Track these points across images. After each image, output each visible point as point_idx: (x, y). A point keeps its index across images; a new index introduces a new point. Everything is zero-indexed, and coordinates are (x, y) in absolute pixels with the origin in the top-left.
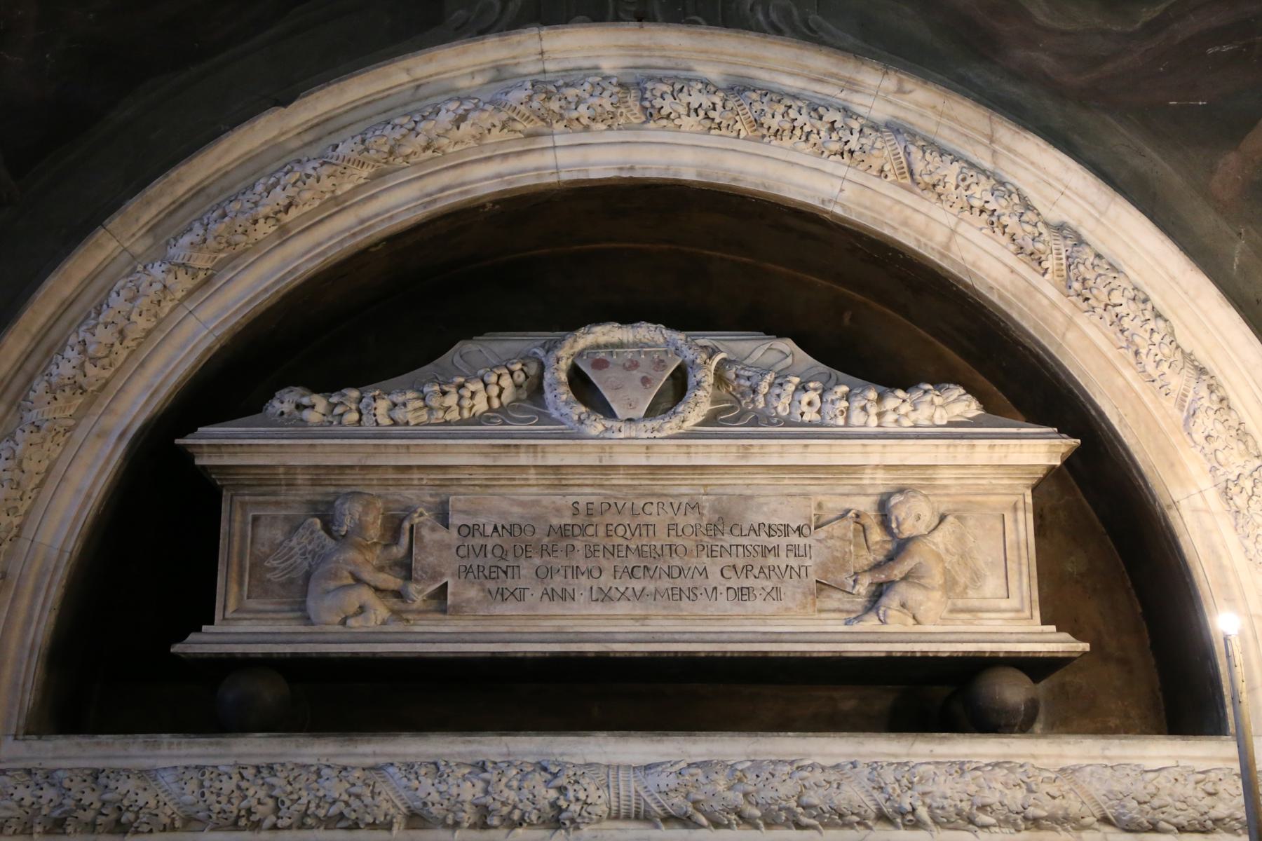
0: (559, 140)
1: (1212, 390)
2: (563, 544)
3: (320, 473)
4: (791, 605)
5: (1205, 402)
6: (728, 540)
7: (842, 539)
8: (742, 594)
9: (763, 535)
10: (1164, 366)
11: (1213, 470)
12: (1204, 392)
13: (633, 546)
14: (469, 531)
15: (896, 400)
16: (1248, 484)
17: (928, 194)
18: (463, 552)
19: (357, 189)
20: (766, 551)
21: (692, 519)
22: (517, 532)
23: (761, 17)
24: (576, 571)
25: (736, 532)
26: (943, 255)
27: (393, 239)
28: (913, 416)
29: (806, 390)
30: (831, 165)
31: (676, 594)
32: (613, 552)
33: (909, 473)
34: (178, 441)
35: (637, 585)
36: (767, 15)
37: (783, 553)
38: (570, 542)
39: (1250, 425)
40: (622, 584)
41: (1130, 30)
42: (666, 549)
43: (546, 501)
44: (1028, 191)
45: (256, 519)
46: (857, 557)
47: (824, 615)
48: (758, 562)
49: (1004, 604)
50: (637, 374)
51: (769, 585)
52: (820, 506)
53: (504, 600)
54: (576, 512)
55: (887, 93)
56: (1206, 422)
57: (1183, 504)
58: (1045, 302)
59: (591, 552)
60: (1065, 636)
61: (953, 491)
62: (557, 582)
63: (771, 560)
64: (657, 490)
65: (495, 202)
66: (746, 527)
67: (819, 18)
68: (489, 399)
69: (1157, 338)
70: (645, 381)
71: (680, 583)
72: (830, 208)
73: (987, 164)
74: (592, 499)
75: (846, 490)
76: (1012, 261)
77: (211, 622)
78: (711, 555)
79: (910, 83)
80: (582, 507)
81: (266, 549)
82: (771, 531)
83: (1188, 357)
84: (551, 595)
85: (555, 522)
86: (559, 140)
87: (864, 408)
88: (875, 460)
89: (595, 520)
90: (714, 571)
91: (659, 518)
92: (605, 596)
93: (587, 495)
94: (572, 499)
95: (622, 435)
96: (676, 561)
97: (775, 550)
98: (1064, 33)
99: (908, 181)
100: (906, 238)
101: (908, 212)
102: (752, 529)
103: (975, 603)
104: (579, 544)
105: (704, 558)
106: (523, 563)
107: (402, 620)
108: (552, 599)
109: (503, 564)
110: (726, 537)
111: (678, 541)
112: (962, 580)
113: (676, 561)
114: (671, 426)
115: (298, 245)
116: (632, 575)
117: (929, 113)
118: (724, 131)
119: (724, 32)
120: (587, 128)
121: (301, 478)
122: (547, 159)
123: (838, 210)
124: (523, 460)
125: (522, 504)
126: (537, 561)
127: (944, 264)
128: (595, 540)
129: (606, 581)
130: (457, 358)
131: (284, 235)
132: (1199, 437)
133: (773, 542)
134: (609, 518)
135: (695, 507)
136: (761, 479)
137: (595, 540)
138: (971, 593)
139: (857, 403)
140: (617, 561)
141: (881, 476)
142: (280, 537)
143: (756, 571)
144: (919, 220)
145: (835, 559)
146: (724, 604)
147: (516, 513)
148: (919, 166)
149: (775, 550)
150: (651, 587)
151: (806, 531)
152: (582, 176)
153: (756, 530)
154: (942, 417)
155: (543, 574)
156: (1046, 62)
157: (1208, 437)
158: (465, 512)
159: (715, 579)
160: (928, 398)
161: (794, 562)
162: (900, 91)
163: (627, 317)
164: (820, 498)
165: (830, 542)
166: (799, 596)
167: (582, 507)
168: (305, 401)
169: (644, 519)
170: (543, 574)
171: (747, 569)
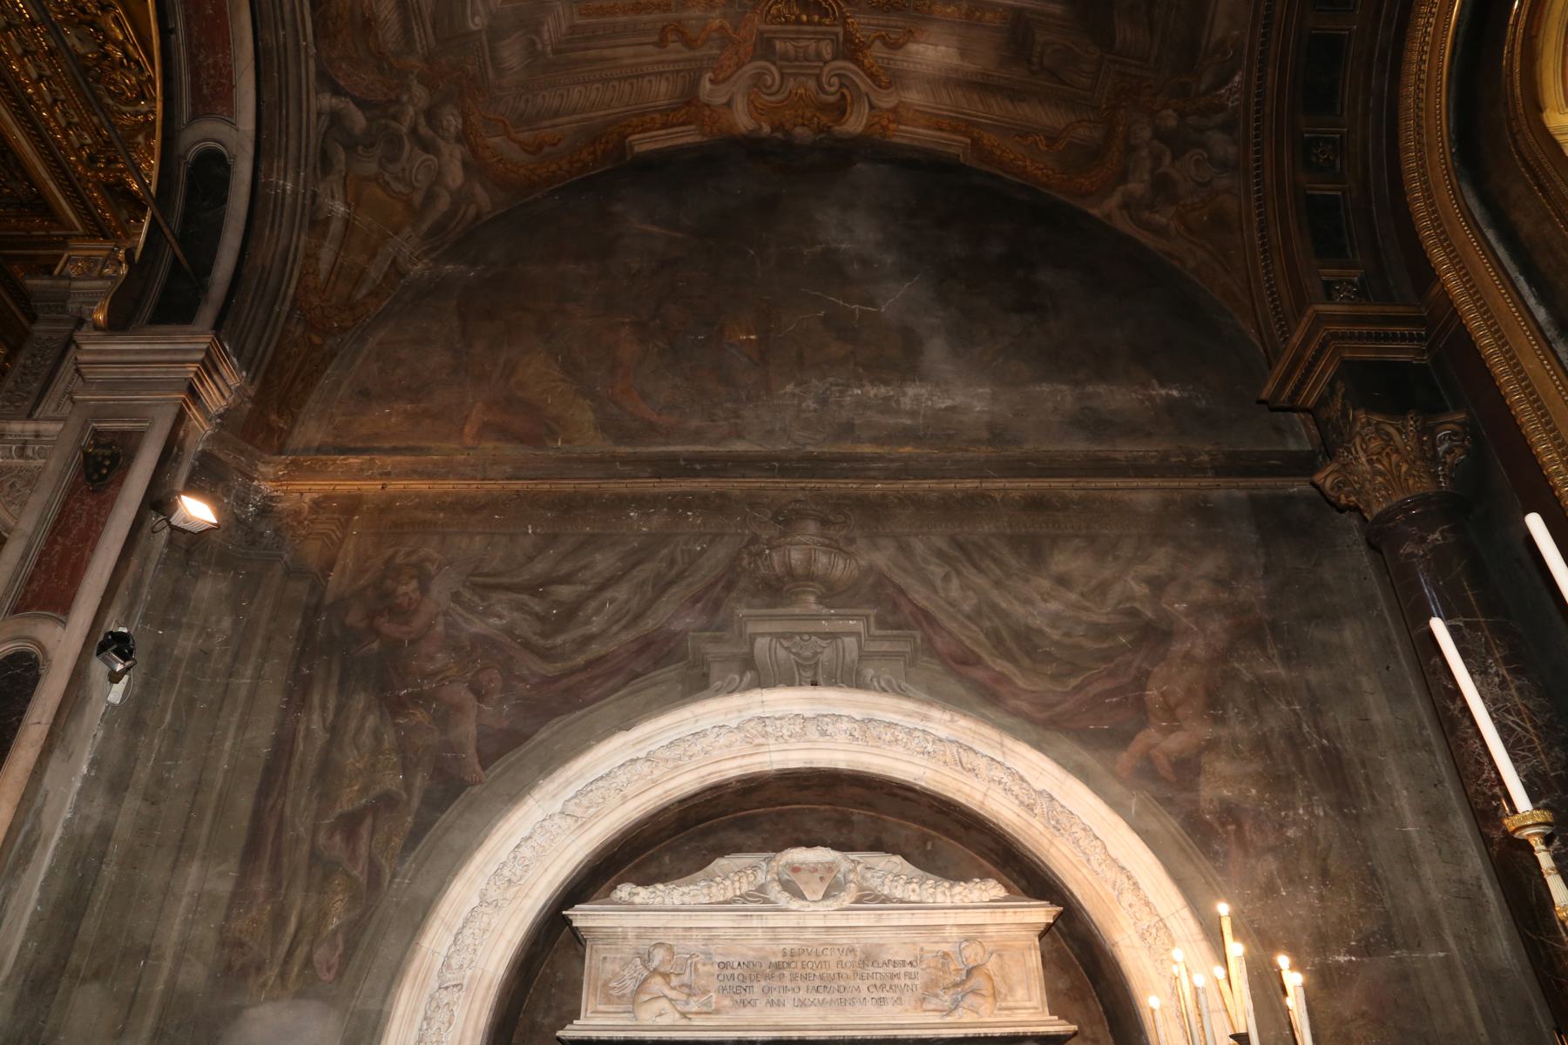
0: (772, 748)
1: (1129, 878)
2: (777, 973)
3: (642, 933)
4: (909, 1008)
5: (1126, 885)
6: (871, 970)
7: (935, 968)
8: (881, 1001)
9: (891, 967)
10: (1103, 866)
11: (1135, 924)
12: (1125, 880)
13: (817, 974)
14: (724, 965)
15: (959, 888)
16: (1154, 931)
17: (969, 774)
18: (721, 978)
19: (663, 775)
20: (893, 976)
21: (850, 958)
22: (751, 965)
23: (876, 684)
24: (785, 989)
25: (875, 965)
26: (981, 808)
27: (682, 801)
28: (970, 896)
29: (910, 883)
30: (918, 759)
31: (842, 1002)
32: (806, 977)
33: (970, 929)
34: (564, 912)
35: (820, 997)
36: (879, 683)
37: (902, 976)
38: (782, 971)
39: (1151, 899)
40: (812, 996)
41: (1065, 690)
42: (836, 976)
43: (768, 948)
44: (1022, 773)
45: (605, 958)
46: (944, 979)
47: (927, 1014)
48: (888, 983)
49: (1028, 1004)
50: (818, 875)
51: (895, 996)
52: (922, 949)
53: (745, 1006)
54: (784, 955)
55: (945, 721)
56: (1129, 897)
57: (1121, 943)
58: (1037, 832)
59: (794, 978)
60: (1063, 1022)
61: (995, 939)
62: (775, 996)
63: (896, 981)
64: (831, 941)
65: (738, 781)
66: (881, 961)
67: (907, 685)
68: (734, 889)
69: (1097, 850)
70: (822, 879)
71: (845, 995)
72: (919, 783)
73: (999, 759)
74: (794, 946)
75: (936, 939)
76: (1018, 810)
77: (579, 1019)
78: (862, 978)
79: (957, 717)
80: (788, 951)
81: (610, 976)
82: (895, 964)
83: (1114, 861)
84: (771, 1003)
85: (773, 960)
86: (772, 748)
87: (944, 893)
88: (951, 921)
89: (795, 959)
90: (864, 987)
91: (831, 957)
92: (802, 1004)
93: (790, 944)
94: (782, 947)
95: (811, 909)
96: (842, 983)
97: (897, 975)
98: (1033, 692)
99: (959, 768)
100: (960, 798)
101: (961, 785)
102: (884, 963)
103: (1011, 1004)
104: (786, 973)
105: (858, 981)
106: (756, 985)
107: (686, 1017)
108: (772, 1005)
109: (744, 985)
110: (870, 968)
111: (843, 971)
112: (1004, 991)
113: (842, 983)
114: (833, 904)
115: (632, 805)
116: (817, 991)
117: (968, 732)
118: (860, 742)
119: (858, 691)
120: (786, 742)
121: (631, 935)
122: (766, 758)
123: (923, 784)
124: (755, 923)
125: (754, 950)
126: (763, 983)
127: (982, 812)
128: (795, 971)
129: (802, 994)
130: (716, 869)
131: (625, 800)
132: (1125, 904)
133: (897, 970)
134: (804, 958)
135: (852, 950)
136: (888, 934)
137: (795, 971)
138: (1009, 998)
139: (940, 889)
140: (809, 983)
141: (955, 930)
142: (618, 969)
143: (888, 988)
144: (967, 789)
145: (932, 980)
146: (871, 1007)
147: (750, 956)
148: (964, 760)
149: (897, 975)
150: (828, 998)
151: (914, 964)
152: (785, 767)
153: (886, 964)
154: (986, 897)
155: (767, 991)
156: (1025, 706)
157: (1130, 905)
158: (721, 954)
159: (864, 993)
160: (978, 886)
161: (908, 982)
162: (952, 721)
163: (810, 845)
164: (922, 945)
165: (929, 970)
166: (913, 1003)
167: (788, 951)
168: (635, 891)
169: (822, 958)
170: (767, 991)
171: (883, 987)
